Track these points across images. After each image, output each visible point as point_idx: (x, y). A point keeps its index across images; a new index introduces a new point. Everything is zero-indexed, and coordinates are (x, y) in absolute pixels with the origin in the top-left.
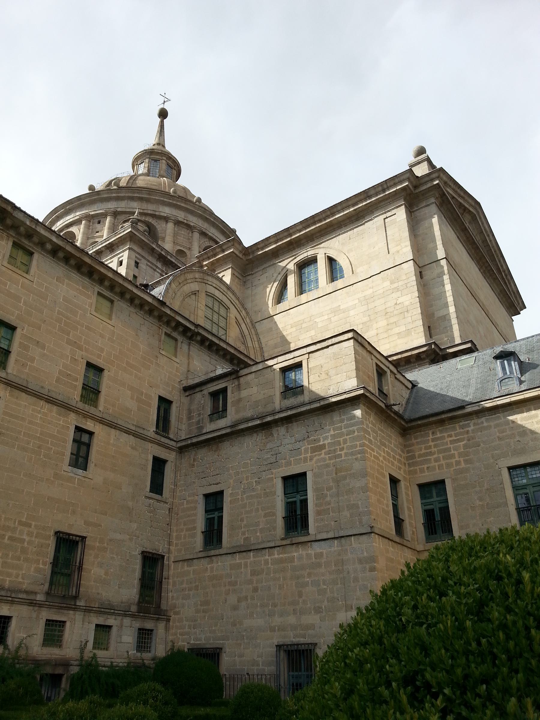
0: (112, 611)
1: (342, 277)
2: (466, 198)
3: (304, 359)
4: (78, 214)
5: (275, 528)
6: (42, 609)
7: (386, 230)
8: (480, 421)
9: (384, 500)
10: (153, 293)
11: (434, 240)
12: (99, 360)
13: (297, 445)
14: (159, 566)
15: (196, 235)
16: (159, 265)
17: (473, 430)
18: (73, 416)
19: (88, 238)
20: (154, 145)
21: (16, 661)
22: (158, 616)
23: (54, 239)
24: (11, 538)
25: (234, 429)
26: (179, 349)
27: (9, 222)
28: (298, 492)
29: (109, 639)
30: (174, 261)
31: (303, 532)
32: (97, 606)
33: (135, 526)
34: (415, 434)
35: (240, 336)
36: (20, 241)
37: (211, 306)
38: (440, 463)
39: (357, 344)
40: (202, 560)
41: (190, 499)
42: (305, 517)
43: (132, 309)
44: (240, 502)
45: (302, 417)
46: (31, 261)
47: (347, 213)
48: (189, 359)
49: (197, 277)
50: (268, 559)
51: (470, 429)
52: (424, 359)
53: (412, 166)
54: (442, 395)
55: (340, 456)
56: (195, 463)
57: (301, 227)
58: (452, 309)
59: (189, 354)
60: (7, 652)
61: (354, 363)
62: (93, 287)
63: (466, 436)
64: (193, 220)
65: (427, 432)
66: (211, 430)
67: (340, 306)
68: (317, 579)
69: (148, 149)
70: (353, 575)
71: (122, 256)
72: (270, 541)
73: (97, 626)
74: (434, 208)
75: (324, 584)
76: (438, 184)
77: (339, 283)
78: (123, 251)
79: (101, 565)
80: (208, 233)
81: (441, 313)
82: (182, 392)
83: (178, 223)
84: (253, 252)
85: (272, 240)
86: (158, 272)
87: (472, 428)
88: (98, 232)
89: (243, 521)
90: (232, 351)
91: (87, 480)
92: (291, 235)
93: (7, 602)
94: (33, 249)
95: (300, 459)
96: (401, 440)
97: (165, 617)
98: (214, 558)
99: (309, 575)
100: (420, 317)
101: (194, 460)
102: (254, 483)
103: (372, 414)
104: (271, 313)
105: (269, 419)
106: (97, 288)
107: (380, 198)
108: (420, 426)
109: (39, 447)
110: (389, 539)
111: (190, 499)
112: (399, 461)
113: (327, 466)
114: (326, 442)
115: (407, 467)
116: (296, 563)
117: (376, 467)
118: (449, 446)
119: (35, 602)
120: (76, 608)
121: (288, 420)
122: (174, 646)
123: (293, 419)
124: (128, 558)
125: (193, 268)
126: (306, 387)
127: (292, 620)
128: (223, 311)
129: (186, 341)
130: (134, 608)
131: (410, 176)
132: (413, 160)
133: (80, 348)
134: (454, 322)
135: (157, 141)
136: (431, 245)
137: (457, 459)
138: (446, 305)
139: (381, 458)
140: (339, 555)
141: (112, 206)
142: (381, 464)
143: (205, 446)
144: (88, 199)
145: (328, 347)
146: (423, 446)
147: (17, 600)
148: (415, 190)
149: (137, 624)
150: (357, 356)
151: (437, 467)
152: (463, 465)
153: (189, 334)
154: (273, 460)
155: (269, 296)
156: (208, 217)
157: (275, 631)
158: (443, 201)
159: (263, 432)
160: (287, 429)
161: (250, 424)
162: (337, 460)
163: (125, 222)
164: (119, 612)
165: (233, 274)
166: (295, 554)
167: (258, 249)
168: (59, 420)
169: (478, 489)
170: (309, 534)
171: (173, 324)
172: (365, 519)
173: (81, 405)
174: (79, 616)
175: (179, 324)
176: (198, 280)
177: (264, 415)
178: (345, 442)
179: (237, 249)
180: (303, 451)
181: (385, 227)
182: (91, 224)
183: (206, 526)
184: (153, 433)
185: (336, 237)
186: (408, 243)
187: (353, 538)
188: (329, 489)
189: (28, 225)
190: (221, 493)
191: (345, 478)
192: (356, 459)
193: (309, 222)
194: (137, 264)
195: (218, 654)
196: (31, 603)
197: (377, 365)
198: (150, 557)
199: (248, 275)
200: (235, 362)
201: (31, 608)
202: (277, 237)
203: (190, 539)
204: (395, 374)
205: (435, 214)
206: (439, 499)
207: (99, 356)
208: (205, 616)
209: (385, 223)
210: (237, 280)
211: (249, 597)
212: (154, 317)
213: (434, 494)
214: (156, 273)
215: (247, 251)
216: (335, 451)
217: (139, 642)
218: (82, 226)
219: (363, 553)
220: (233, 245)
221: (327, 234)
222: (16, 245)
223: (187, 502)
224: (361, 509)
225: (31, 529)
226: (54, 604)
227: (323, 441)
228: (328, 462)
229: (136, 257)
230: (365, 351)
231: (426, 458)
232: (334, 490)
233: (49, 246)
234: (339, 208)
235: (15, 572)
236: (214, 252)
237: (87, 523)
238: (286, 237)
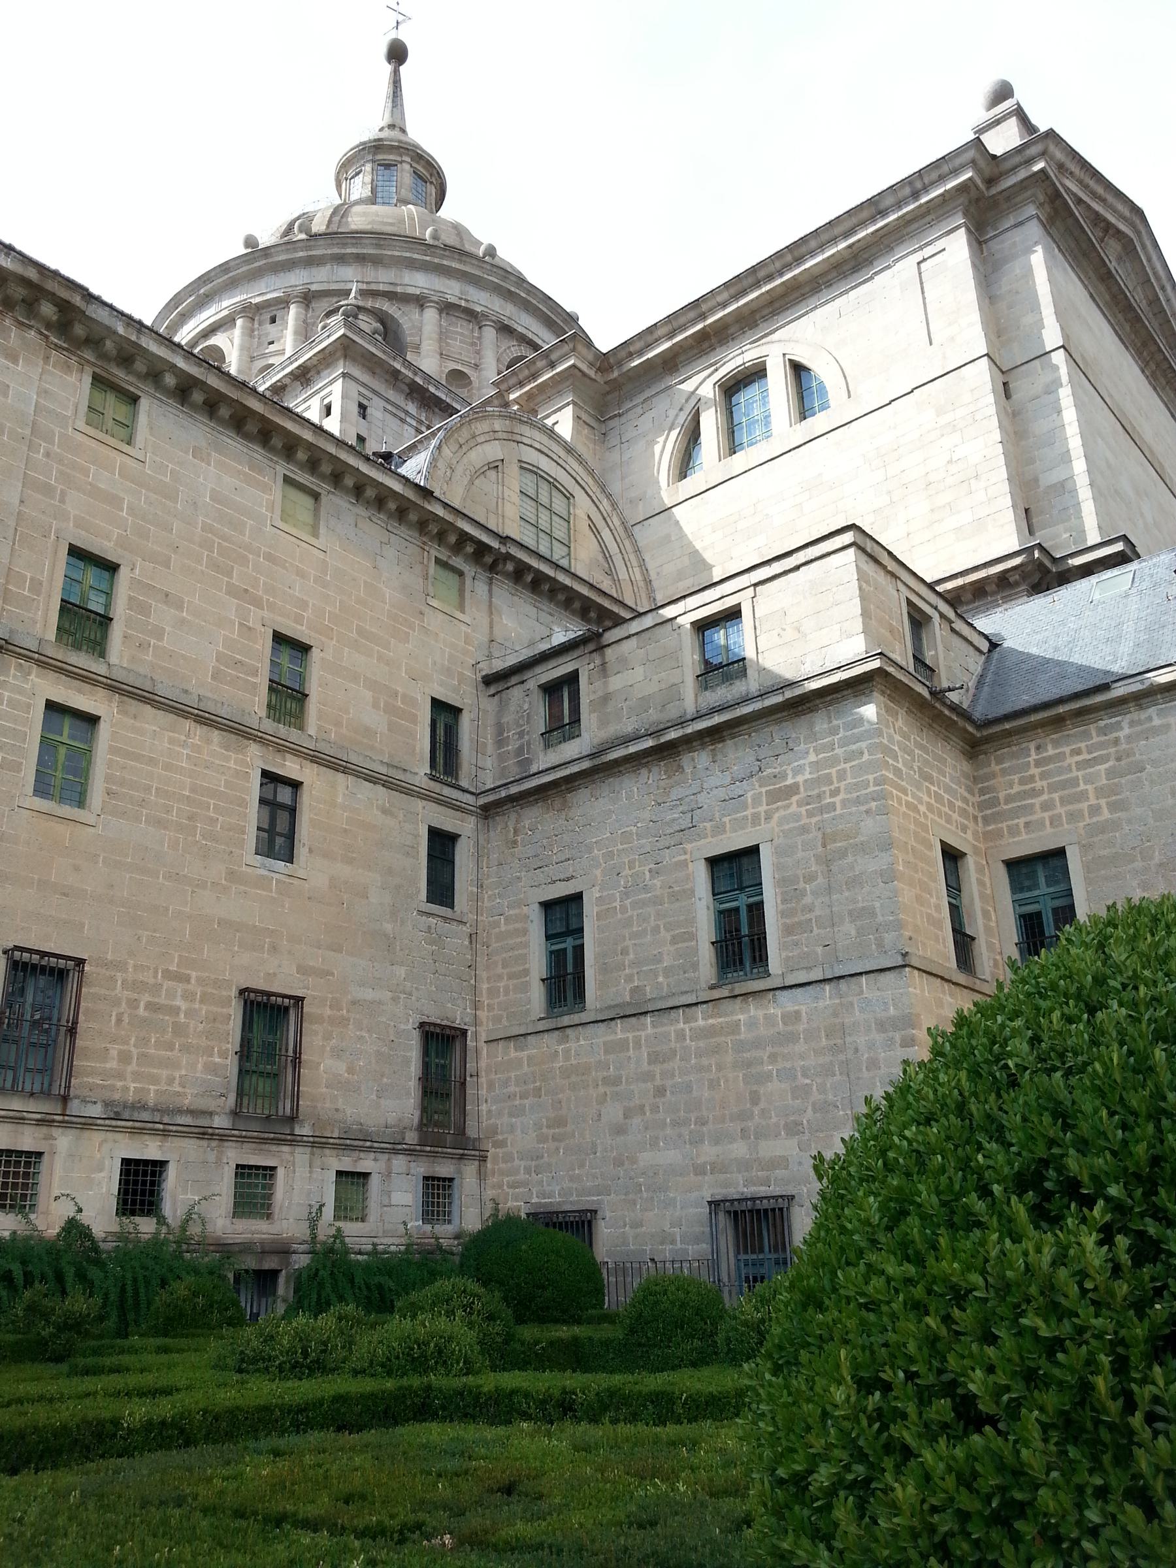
0: (368, 1144)
1: (824, 407)
2: (1110, 199)
3: (744, 599)
4: (225, 304)
5: (695, 966)
6: (226, 1144)
7: (922, 289)
8: (1143, 715)
9: (931, 896)
10: (403, 471)
11: (1035, 307)
12: (299, 627)
13: (737, 789)
14: (458, 1053)
15: (490, 333)
16: (412, 408)
17: (1128, 737)
18: (254, 749)
19: (252, 359)
20: (381, 130)
21: (184, 1247)
22: (461, 1152)
23: (181, 363)
24: (150, 1006)
25: (597, 761)
26: (467, 594)
27: (79, 330)
28: (741, 889)
29: (365, 1199)
30: (443, 397)
31: (755, 971)
32: (336, 1135)
33: (401, 972)
34: (999, 753)
35: (600, 557)
36: (107, 371)
37: (532, 493)
38: (1055, 812)
39: (864, 558)
40: (546, 1035)
41: (511, 912)
42: (759, 939)
43: (361, 511)
44: (619, 916)
45: (746, 727)
46: (135, 415)
47: (833, 255)
48: (491, 613)
49: (497, 427)
50: (683, 1030)
51: (1121, 734)
52: (1017, 584)
53: (982, 130)
54: (1059, 663)
55: (832, 807)
56: (519, 838)
57: (725, 296)
58: (1079, 466)
59: (490, 602)
60: (164, 1230)
61: (857, 601)
62: (272, 465)
63: (1112, 750)
64: (481, 300)
65: (1024, 745)
66: (549, 765)
68: (788, 1065)
69: (370, 141)
70: (866, 1056)
71: (330, 394)
72: (686, 992)
73: (339, 1173)
74: (1034, 229)
75: (805, 1075)
76: (1042, 170)
77: (818, 422)
78: (331, 383)
79: (338, 1053)
80: (515, 326)
81: (1054, 477)
82: (481, 686)
83: (447, 308)
84: (620, 364)
85: (661, 332)
86: (411, 425)
87: (1127, 731)
88: (272, 343)
89: (627, 954)
90: (584, 591)
91: (296, 882)
92: (703, 316)
93: (154, 1132)
94: (138, 388)
95: (745, 818)
96: (966, 766)
97: (477, 1153)
98: (569, 1031)
99: (773, 1058)
100: (1005, 487)
101: (516, 832)
102: (647, 873)
103: (902, 713)
104: (666, 501)
105: (673, 735)
106: (282, 468)
107: (907, 213)
108: (1009, 733)
109: (190, 818)
110: (942, 978)
111: (511, 912)
112: (963, 813)
113: (804, 830)
114: (800, 779)
115: (980, 824)
116: (744, 1034)
117: (912, 827)
118: (1074, 774)
119: (210, 1131)
120: (294, 1141)
121: (715, 735)
122: (497, 1210)
123: (725, 733)
124: (392, 1038)
125: (488, 409)
126: (751, 660)
127: (739, 1149)
128: (559, 504)
129: (483, 575)
130: (412, 1138)
131: (978, 156)
132: (982, 115)
133: (257, 602)
134: (1085, 494)
135: (387, 120)
136: (1028, 319)
137: (1093, 801)
138: (1066, 458)
139: (922, 808)
140: (835, 1015)
141: (298, 279)
142: (922, 820)
143: (536, 801)
144: (245, 269)
145: (797, 568)
146: (1016, 777)
147: (174, 1128)
148: (988, 188)
149: (421, 1168)
150: (864, 585)
151: (1047, 823)
152: (1106, 814)
153: (489, 559)
154: (685, 822)
155: (659, 463)
156: (513, 289)
157: (705, 1174)
158: (1056, 210)
159: (662, 763)
160: (714, 756)
161: (633, 749)
162: (826, 816)
163: (329, 314)
164: (383, 1145)
165: (577, 418)
166: (741, 1017)
167: (631, 356)
168: (228, 759)
169: (1139, 864)
170: (769, 975)
171: (452, 539)
172: (889, 938)
173: (269, 726)
174: (301, 1155)
175: (464, 537)
176: (500, 435)
177: (662, 726)
178: (842, 776)
179: (583, 358)
180: (750, 800)
181: (922, 283)
182: (256, 326)
183: (550, 966)
184: (426, 779)
185: (807, 313)
186: (975, 317)
187: (864, 978)
188: (810, 878)
189: (121, 336)
190: (578, 898)
191: (843, 853)
192: (867, 812)
193: (745, 283)
194: (363, 408)
195: (590, 1222)
196: (204, 1134)
197: (910, 603)
198: (438, 1034)
199: (610, 418)
200: (593, 615)
201: (205, 1143)
202: (673, 323)
203: (519, 996)
204: (950, 622)
205: (1036, 243)
206: (1052, 890)
207: (299, 619)
208: (557, 1149)
209: (920, 274)
210: (586, 431)
211: (647, 1108)
212: (410, 525)
213: (1042, 880)
214: (406, 427)
215: (605, 362)
216: (819, 797)
217: (425, 1204)
218: (237, 332)
219: (886, 1010)
220: (574, 350)
221: (788, 309)
222: (100, 382)
223: (506, 920)
224: (880, 919)
225: (189, 987)
226: (249, 1134)
227: (793, 777)
228: (805, 821)
229: (360, 394)
230: (882, 573)
231: (1024, 803)
232: (820, 880)
233: (170, 380)
234: (813, 244)
235: (164, 1073)
236: (533, 370)
237: (303, 970)
238: (694, 322)
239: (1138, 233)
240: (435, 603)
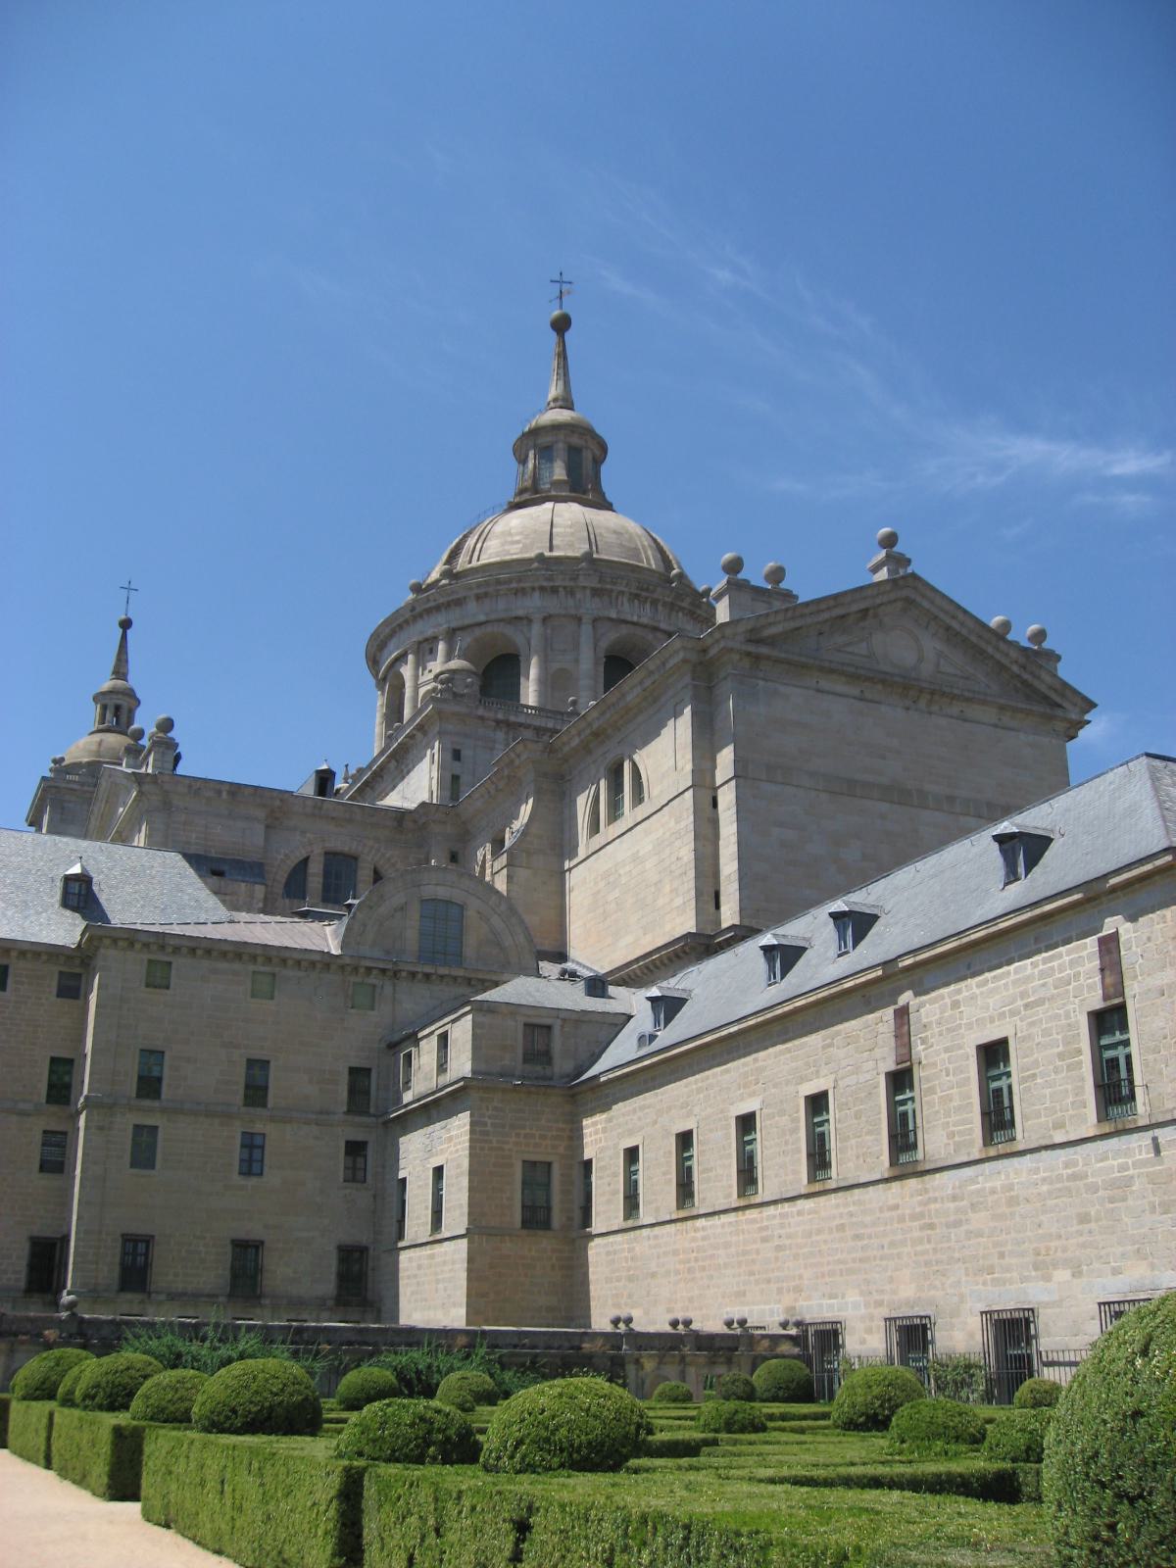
67: (638, 852)
130: (330, 1303)
239: (915, 588)
240: (353, 1011)
